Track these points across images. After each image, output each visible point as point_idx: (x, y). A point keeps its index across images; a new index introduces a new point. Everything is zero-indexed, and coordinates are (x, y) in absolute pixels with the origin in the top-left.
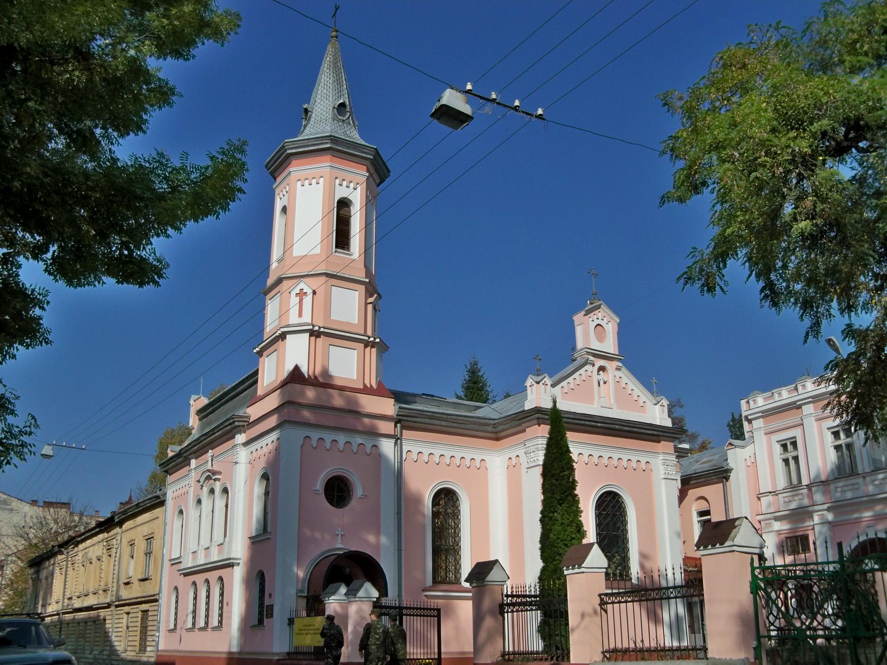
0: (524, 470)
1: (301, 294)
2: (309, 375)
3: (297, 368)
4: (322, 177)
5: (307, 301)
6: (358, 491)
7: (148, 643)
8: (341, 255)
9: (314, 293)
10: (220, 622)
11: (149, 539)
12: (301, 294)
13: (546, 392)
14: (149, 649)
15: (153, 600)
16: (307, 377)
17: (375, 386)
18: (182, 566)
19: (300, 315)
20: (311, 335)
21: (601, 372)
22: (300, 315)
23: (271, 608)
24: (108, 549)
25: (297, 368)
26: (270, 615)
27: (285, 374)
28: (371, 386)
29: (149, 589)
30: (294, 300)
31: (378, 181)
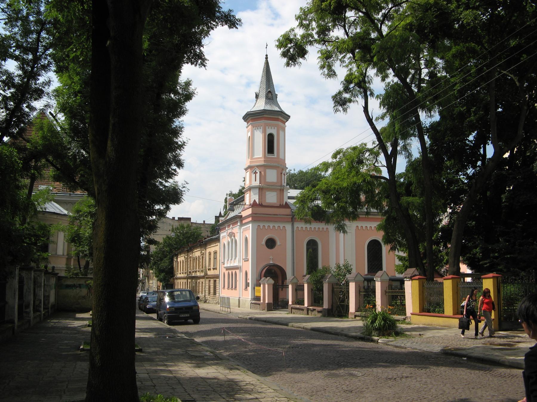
1: (256, 173)
2: (259, 203)
3: (255, 201)
4: (261, 126)
5: (258, 175)
6: (278, 243)
7: (217, 292)
8: (271, 156)
9: (260, 172)
10: (236, 287)
11: (215, 253)
12: (256, 173)
14: (217, 294)
15: (217, 277)
16: (258, 203)
18: (225, 265)
19: (256, 181)
22: (256, 181)
23: (249, 283)
24: (202, 254)
25: (255, 201)
26: (249, 286)
27: (252, 202)
29: (216, 272)
30: (254, 175)
31: (285, 121)
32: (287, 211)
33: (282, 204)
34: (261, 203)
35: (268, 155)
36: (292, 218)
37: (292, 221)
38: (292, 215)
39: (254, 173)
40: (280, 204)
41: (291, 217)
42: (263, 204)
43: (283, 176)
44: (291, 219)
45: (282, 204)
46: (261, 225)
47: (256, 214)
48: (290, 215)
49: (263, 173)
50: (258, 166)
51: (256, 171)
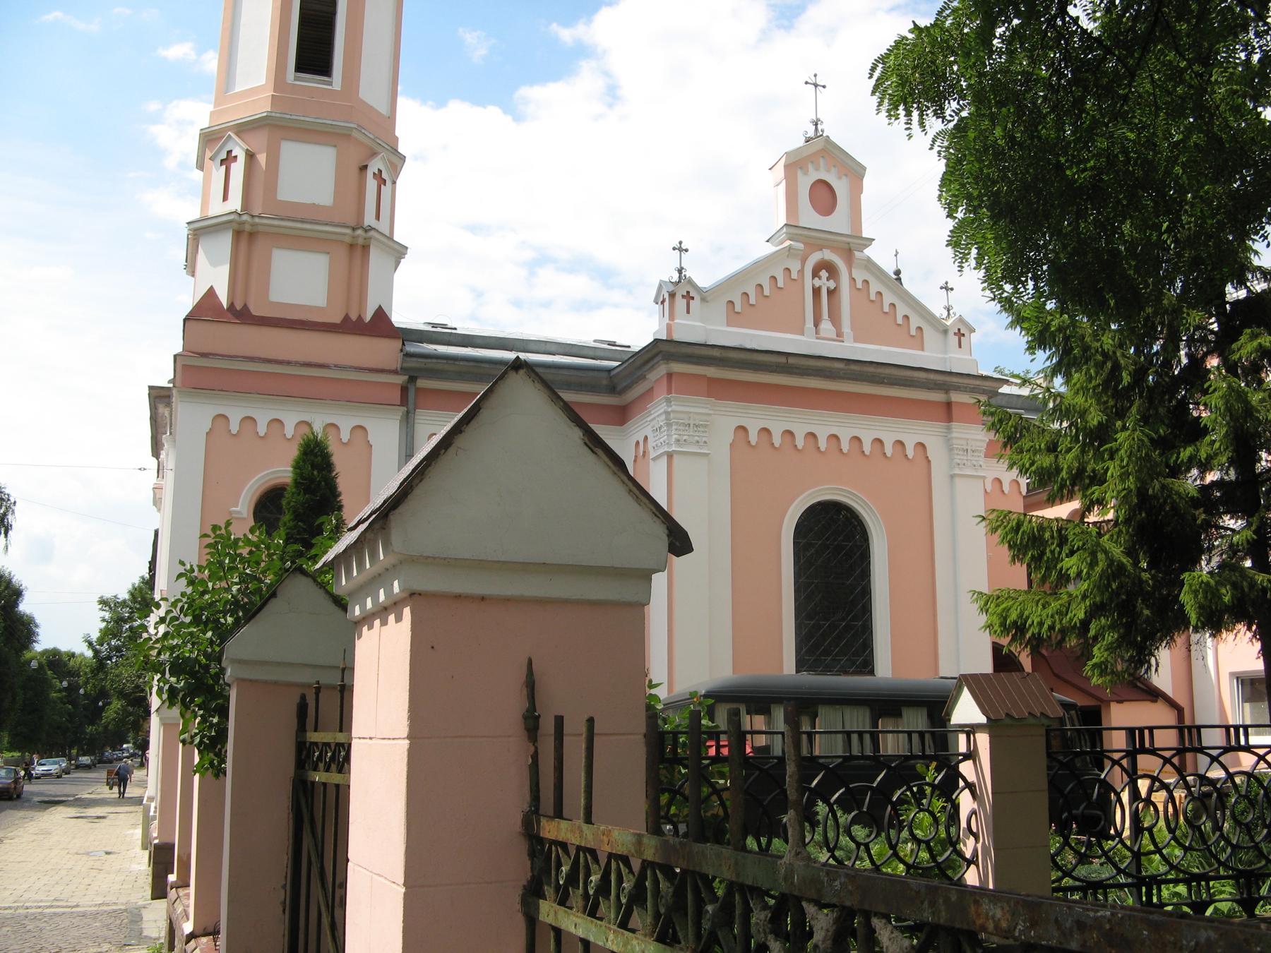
0: (651, 463)
1: (228, 160)
3: (211, 293)
5: (238, 169)
8: (312, 82)
9: (250, 156)
13: (688, 312)
17: (368, 317)
19: (225, 198)
20: (238, 234)
21: (824, 274)
22: (225, 198)
25: (211, 293)
28: (360, 318)
32: (384, 352)
33: (354, 317)
34: (245, 306)
35: (296, 79)
36: (404, 390)
37: (404, 401)
38: (404, 370)
39: (222, 162)
40: (347, 318)
41: (400, 380)
42: (255, 311)
43: (371, 184)
44: (397, 395)
45: (354, 317)
46: (235, 414)
47: (204, 355)
48: (395, 372)
49: (262, 158)
50: (243, 129)
51: (229, 152)
